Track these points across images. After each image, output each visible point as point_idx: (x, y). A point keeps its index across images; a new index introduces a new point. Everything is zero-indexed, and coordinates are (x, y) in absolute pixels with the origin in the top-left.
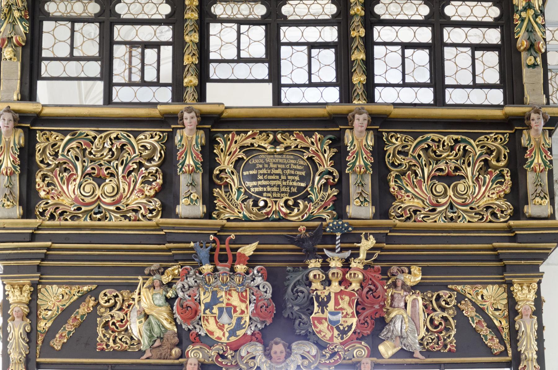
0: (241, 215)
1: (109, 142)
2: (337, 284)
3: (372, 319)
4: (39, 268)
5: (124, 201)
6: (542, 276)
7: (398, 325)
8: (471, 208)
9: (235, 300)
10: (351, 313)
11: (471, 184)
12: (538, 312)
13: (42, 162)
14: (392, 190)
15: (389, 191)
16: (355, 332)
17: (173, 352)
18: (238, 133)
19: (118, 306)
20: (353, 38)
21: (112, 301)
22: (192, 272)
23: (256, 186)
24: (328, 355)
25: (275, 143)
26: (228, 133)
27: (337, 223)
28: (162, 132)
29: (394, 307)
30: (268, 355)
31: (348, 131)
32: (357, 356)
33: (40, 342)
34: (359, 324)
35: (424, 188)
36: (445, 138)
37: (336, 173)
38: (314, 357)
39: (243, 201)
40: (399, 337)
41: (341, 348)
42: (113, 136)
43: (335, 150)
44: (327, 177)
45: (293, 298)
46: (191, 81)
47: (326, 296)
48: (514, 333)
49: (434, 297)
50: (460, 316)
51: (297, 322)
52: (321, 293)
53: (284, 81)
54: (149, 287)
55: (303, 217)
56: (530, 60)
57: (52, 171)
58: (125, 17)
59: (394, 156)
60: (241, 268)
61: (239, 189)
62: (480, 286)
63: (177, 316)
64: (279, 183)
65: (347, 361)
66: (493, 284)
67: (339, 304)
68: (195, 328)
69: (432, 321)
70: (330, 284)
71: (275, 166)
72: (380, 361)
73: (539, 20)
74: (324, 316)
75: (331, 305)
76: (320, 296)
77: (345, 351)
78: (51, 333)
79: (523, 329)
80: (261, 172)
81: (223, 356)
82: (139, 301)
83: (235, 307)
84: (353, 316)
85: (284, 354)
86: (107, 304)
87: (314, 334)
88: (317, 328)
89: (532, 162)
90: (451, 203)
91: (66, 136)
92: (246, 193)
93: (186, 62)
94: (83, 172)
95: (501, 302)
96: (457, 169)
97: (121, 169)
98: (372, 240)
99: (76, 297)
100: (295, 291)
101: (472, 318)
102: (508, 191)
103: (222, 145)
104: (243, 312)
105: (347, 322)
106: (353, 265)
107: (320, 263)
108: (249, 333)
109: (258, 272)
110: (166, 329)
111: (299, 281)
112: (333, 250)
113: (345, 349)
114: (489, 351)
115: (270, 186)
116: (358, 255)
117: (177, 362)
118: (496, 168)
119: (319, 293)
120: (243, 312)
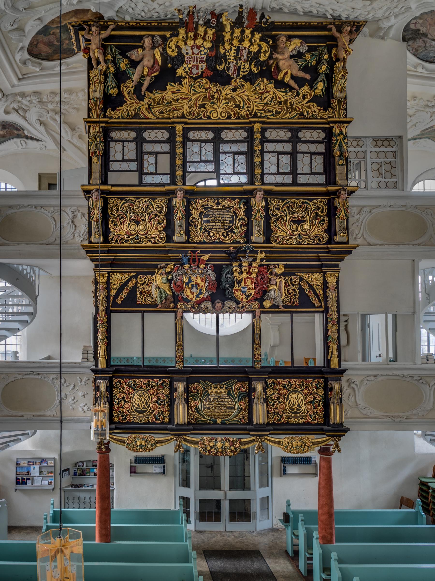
0: (202, 240)
1: (142, 204)
4: (111, 266)
5: (149, 233)
6: (340, 270)
7: (272, 293)
8: (309, 237)
9: (199, 281)
11: (309, 224)
12: (337, 288)
13: (111, 214)
14: (272, 227)
15: (270, 228)
16: (253, 296)
17: (171, 305)
18: (201, 199)
19: (146, 283)
20: (255, 150)
21: (143, 281)
22: (180, 268)
23: (209, 226)
24: (241, 307)
25: (218, 204)
26: (197, 199)
28: (166, 198)
29: (271, 285)
30: (213, 307)
31: (253, 199)
33: (111, 300)
35: (287, 226)
36: (298, 201)
37: (246, 220)
38: (234, 308)
39: (203, 233)
42: (144, 201)
43: (246, 207)
44: (242, 221)
46: (180, 174)
48: (326, 297)
49: (289, 279)
50: (301, 289)
51: (227, 291)
53: (222, 172)
54: (160, 274)
55: (231, 241)
56: (341, 162)
57: (116, 218)
58: (148, 139)
59: (273, 210)
60: (202, 266)
61: (201, 227)
62: (310, 274)
63: (173, 288)
64: (219, 224)
66: (316, 273)
68: (181, 294)
69: (288, 291)
70: (242, 274)
71: (218, 216)
72: (264, 310)
73: (346, 141)
74: (239, 289)
75: (243, 284)
78: (116, 296)
79: (331, 296)
80: (212, 219)
81: (193, 307)
82: (156, 280)
83: (199, 284)
84: (253, 289)
86: (141, 282)
89: (340, 215)
90: (299, 234)
91: (122, 200)
92: (204, 229)
93: (177, 163)
94: (130, 218)
95: (320, 281)
96: (303, 217)
97: (147, 217)
99: (127, 279)
101: (306, 289)
102: (326, 228)
103: (194, 205)
104: (202, 286)
106: (254, 265)
108: (205, 296)
109: (210, 268)
110: (168, 295)
111: (228, 272)
112: (244, 257)
114: (313, 306)
115: (216, 226)
116: (256, 260)
117: (172, 309)
118: (321, 216)
120: (202, 286)
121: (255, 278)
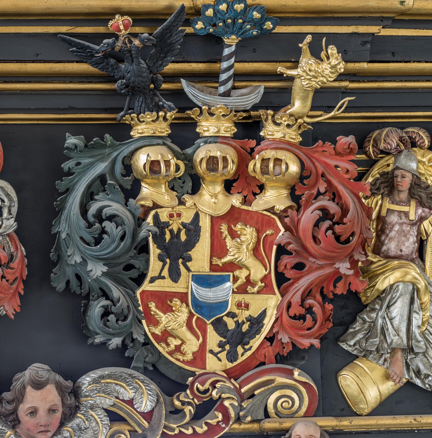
2: (219, 188)
3: (324, 296)
10: (262, 281)
16: (270, 339)
24: (189, 410)
27: (230, 7)
29: (388, 257)
32: (278, 414)
34: (285, 317)
38: (148, 416)
40: (403, 350)
41: (229, 390)
45: (88, 238)
47: (184, 225)
52: (171, 216)
65: (250, 426)
67: (224, 252)
76: (167, 225)
77: (242, 398)
85: (59, 415)
87: (147, 343)
88: (156, 323)
98: (334, 62)
100: (94, 216)
105: (247, 306)
107: (169, 122)
111: (102, 178)
113: (243, 390)
119: (164, 217)
121: (282, 215)
